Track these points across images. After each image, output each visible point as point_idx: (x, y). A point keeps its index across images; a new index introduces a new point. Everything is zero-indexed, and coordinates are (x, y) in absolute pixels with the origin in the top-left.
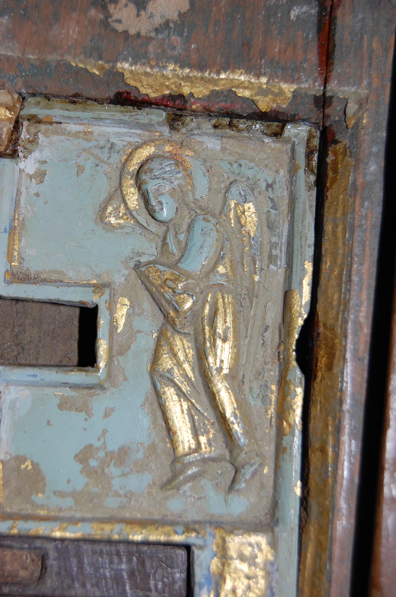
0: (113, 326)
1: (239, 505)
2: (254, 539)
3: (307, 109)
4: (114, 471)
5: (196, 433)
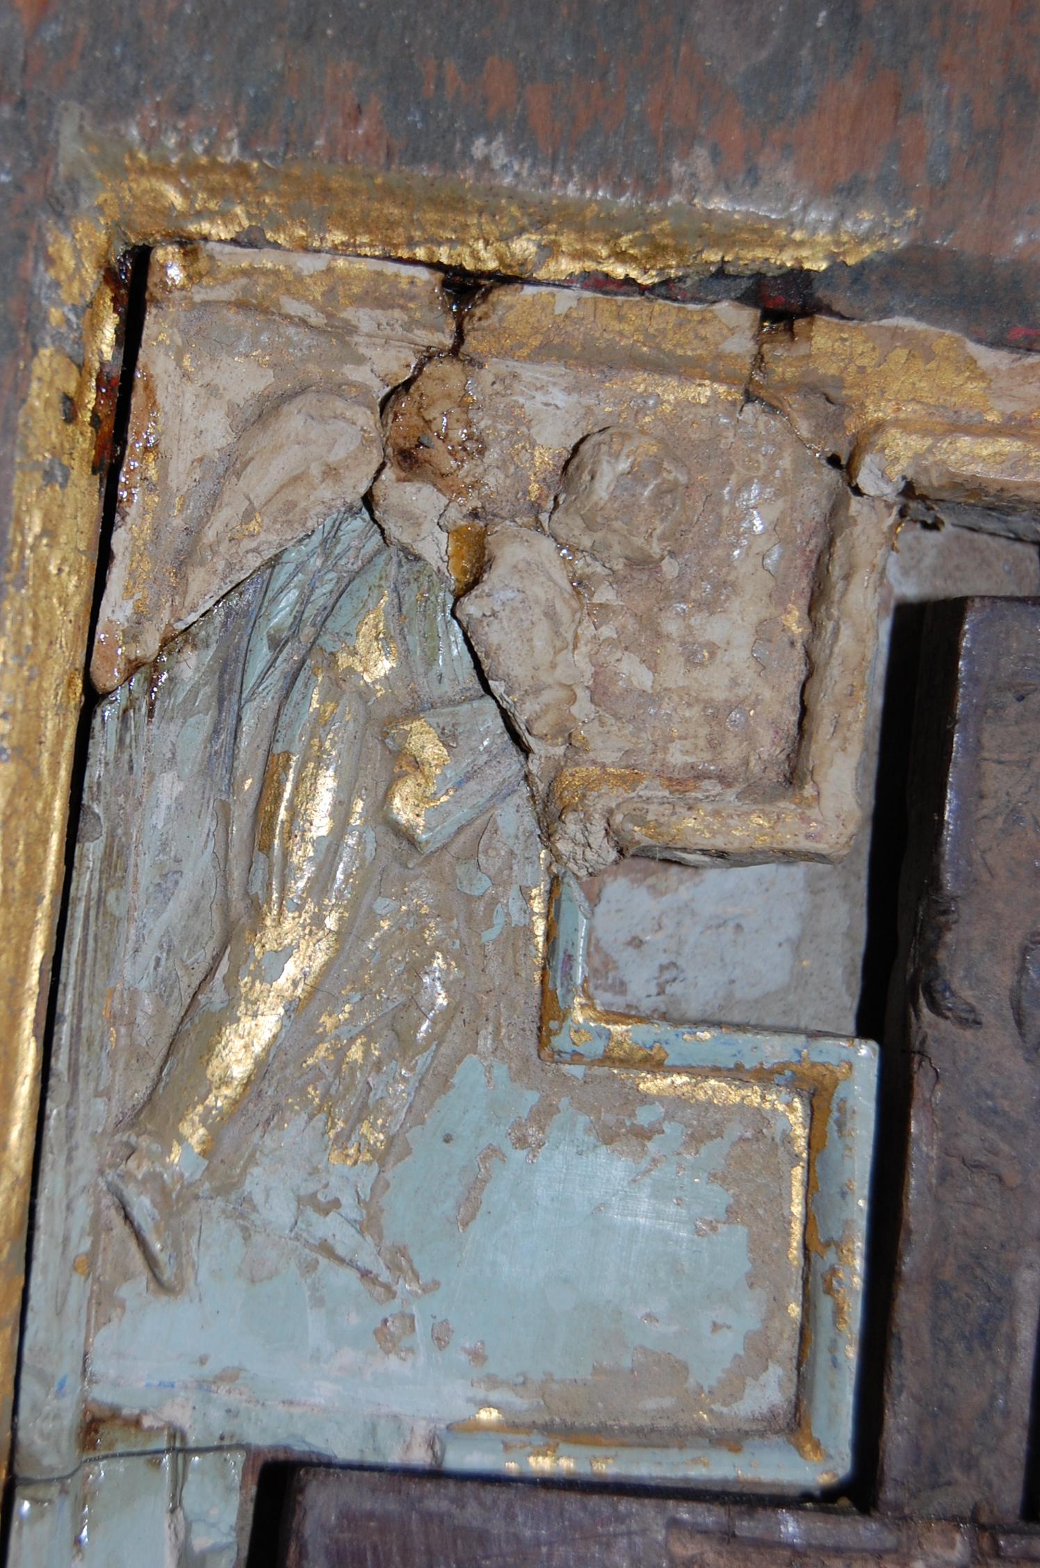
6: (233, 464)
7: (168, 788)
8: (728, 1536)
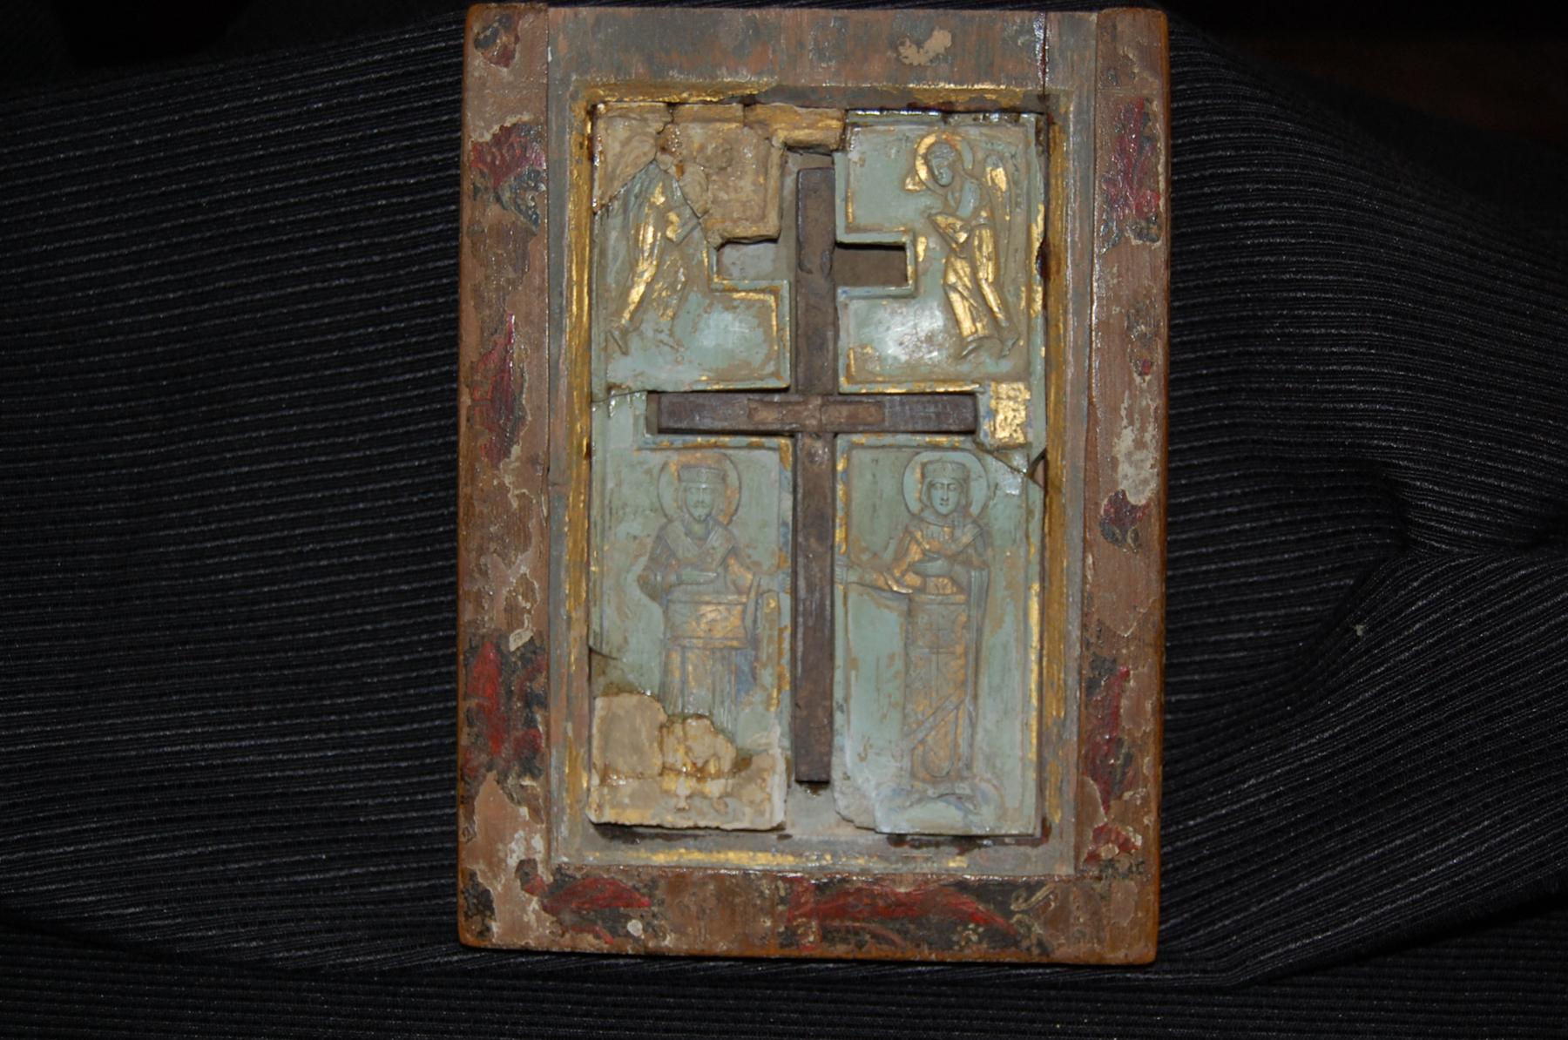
0: (916, 256)
1: (1005, 366)
2: (1015, 386)
3: (1035, 104)
5: (974, 321)
6: (621, 155)
7: (614, 235)
8: (761, 401)
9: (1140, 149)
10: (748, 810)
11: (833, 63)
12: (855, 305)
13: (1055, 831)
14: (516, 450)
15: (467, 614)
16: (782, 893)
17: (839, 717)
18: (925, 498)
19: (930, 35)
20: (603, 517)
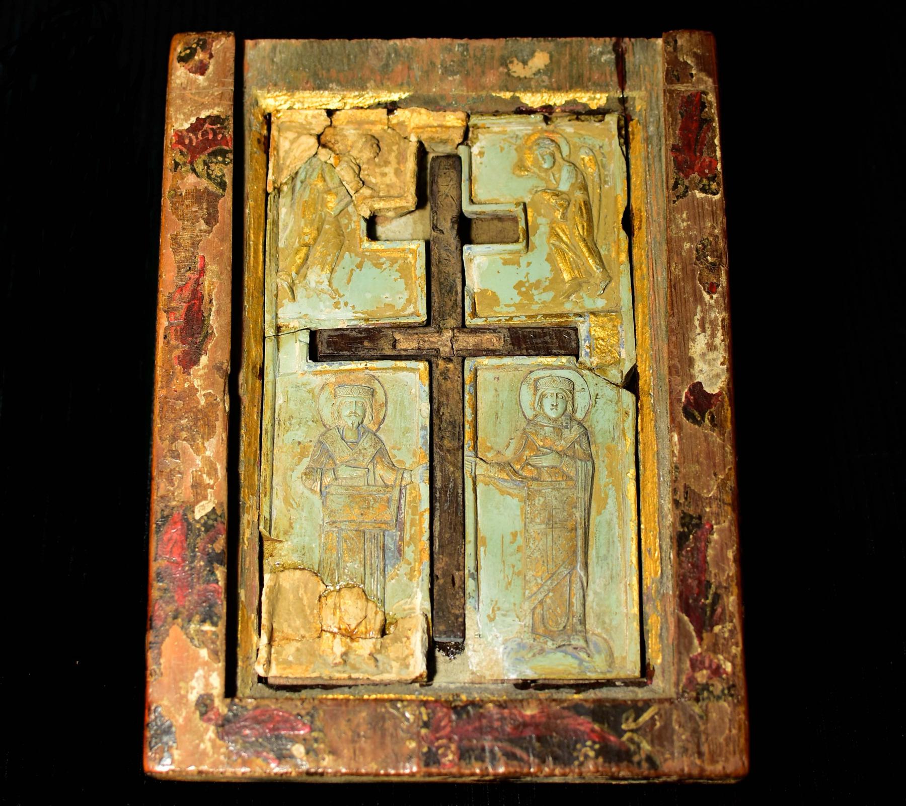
3: (616, 105)
4: (534, 292)
7: (283, 211)
9: (701, 128)
10: (394, 664)
11: (458, 77)
12: (477, 261)
13: (658, 672)
14: (204, 360)
15: (160, 487)
16: (425, 718)
17: (470, 584)
18: (538, 409)
19: (532, 54)
20: (273, 425)
